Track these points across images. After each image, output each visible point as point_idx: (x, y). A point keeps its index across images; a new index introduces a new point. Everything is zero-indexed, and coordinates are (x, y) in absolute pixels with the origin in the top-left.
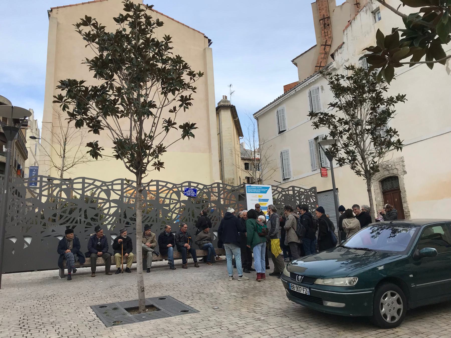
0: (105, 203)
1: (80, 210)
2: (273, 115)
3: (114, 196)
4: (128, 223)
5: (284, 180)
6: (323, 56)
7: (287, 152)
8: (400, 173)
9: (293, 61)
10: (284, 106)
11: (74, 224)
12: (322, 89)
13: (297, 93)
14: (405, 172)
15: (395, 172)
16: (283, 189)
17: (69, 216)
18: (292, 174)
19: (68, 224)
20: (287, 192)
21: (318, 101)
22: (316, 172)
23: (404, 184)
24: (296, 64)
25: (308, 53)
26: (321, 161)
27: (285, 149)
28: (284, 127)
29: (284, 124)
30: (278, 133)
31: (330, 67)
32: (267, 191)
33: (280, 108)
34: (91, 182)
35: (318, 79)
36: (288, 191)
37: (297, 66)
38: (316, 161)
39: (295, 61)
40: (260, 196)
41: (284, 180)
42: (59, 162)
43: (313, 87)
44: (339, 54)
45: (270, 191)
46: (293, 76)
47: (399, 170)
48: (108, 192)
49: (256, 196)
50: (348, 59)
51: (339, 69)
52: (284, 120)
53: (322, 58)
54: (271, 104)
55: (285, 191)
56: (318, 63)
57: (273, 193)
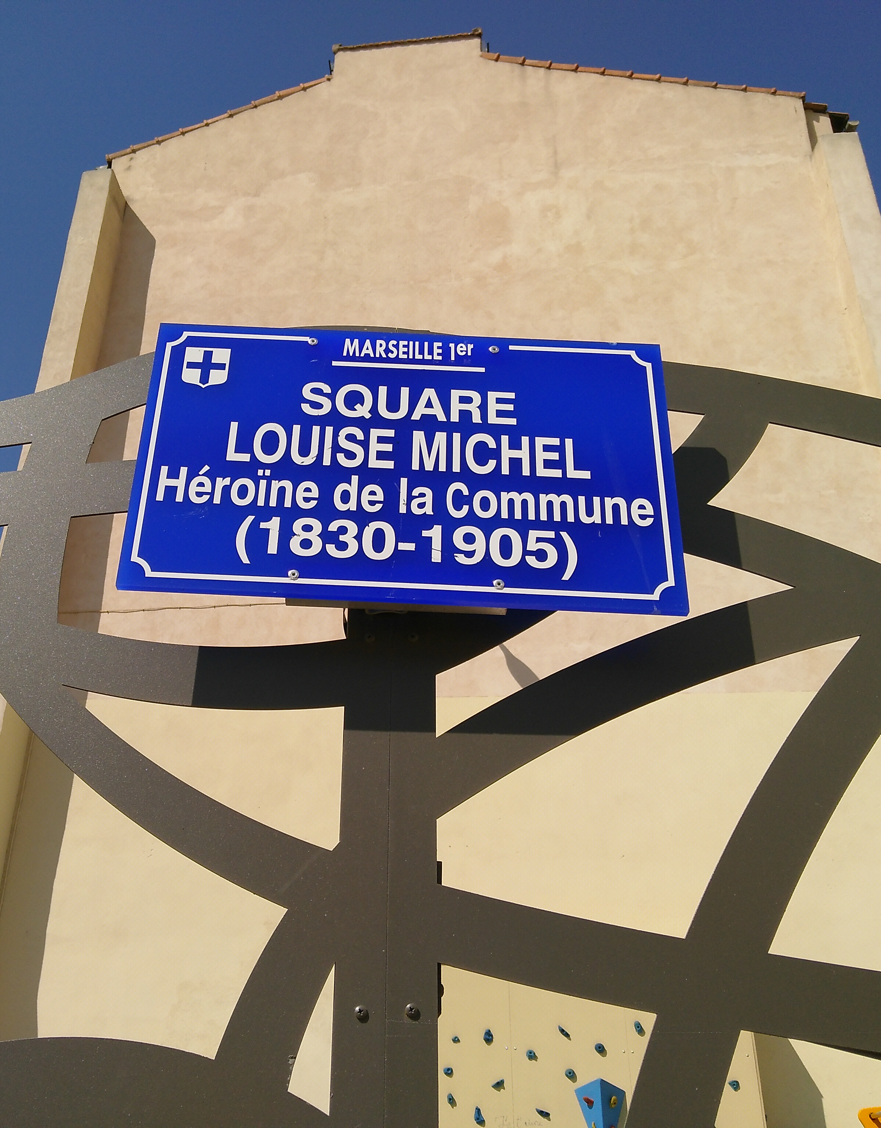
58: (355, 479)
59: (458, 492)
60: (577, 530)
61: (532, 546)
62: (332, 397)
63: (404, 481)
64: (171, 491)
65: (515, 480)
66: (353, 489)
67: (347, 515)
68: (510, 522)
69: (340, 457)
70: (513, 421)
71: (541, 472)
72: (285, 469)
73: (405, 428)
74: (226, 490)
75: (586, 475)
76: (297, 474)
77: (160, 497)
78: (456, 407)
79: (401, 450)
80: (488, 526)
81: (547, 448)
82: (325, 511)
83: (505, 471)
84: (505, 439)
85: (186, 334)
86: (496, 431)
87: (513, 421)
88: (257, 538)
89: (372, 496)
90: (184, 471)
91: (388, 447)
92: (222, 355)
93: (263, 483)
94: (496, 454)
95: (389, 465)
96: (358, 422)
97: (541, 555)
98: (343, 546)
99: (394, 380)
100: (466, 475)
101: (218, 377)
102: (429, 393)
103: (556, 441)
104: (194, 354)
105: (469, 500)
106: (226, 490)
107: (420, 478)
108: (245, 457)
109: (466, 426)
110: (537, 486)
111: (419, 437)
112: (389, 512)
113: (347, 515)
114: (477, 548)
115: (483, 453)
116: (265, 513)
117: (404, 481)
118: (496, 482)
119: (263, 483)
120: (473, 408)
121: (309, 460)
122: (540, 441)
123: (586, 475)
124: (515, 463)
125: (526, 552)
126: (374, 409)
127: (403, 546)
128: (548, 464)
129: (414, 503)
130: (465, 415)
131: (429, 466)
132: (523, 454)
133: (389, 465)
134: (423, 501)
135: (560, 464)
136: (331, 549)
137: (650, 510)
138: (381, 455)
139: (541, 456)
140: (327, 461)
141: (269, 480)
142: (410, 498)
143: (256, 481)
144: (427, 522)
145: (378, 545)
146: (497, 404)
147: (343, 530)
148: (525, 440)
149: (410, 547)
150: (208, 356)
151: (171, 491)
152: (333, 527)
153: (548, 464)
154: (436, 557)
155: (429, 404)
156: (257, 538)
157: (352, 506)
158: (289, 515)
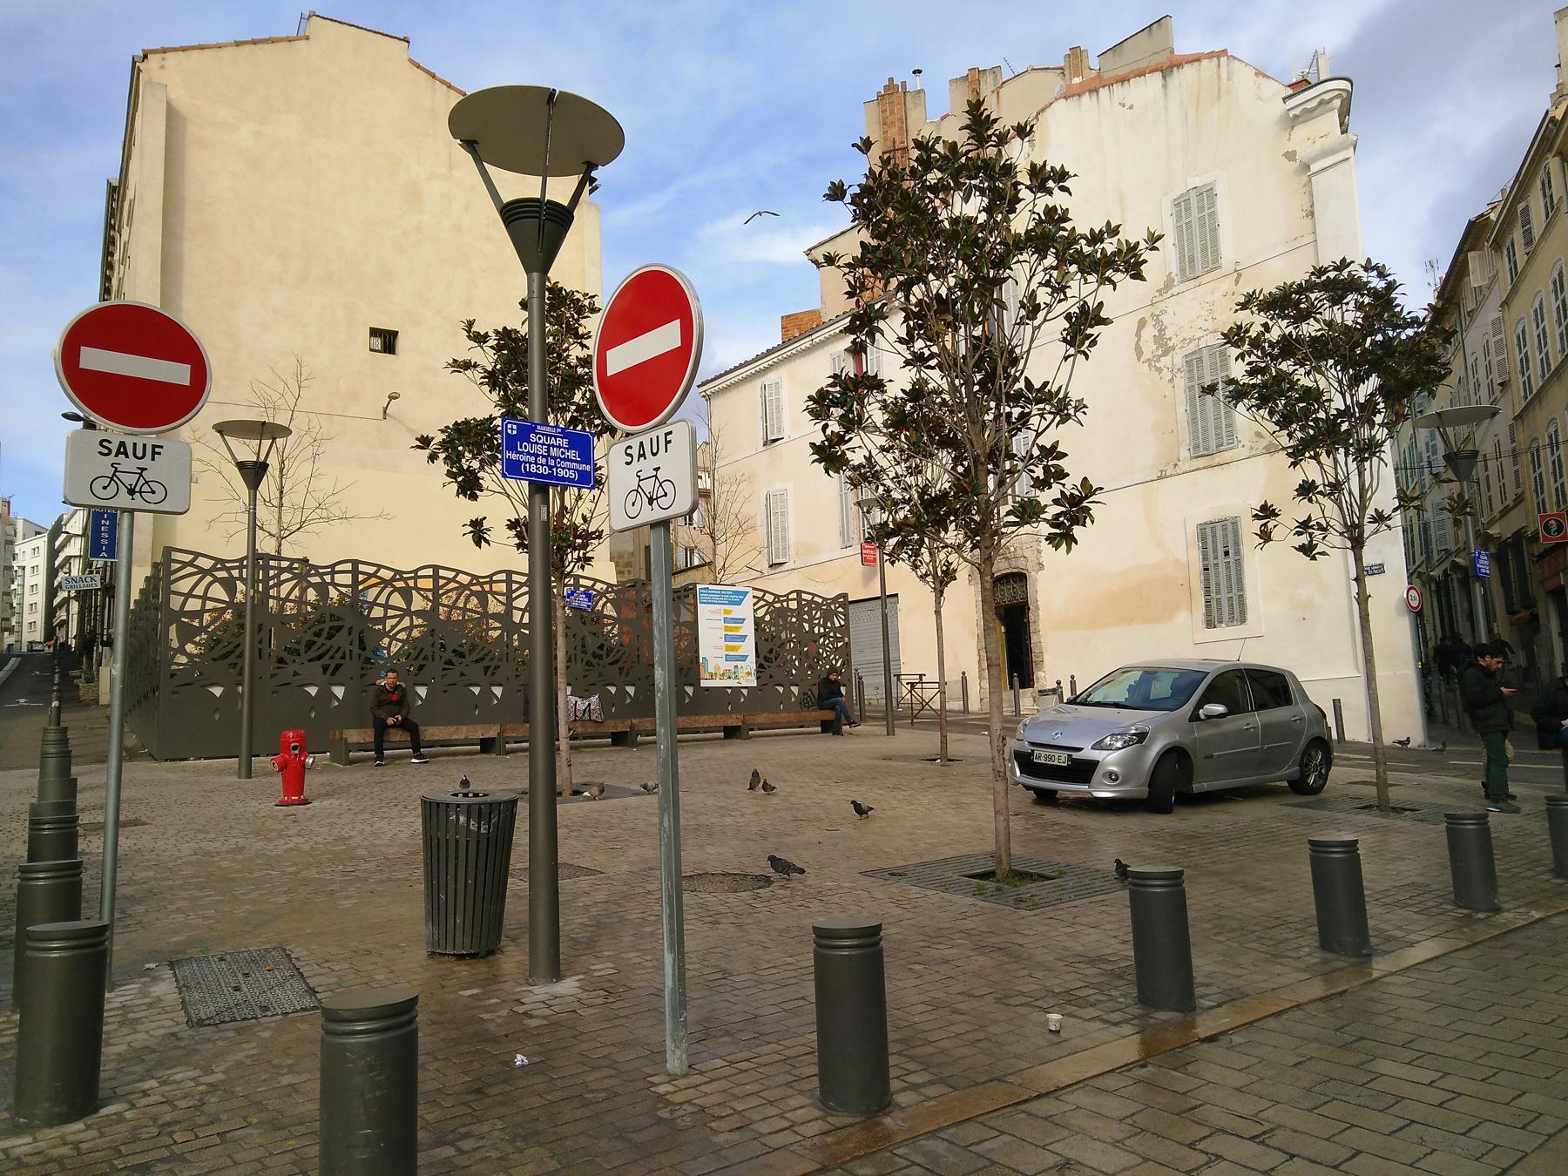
0: (402, 618)
3: (418, 603)
4: (450, 662)
7: (783, 495)
8: (1030, 566)
11: (337, 661)
13: (815, 347)
14: (1041, 566)
15: (1021, 563)
17: (329, 643)
18: (792, 552)
19: (325, 661)
22: (849, 551)
27: (778, 486)
33: (770, 378)
34: (372, 570)
40: (726, 612)
48: (406, 594)
49: (718, 612)
54: (747, 363)
65: (568, 460)
114: (562, 473)
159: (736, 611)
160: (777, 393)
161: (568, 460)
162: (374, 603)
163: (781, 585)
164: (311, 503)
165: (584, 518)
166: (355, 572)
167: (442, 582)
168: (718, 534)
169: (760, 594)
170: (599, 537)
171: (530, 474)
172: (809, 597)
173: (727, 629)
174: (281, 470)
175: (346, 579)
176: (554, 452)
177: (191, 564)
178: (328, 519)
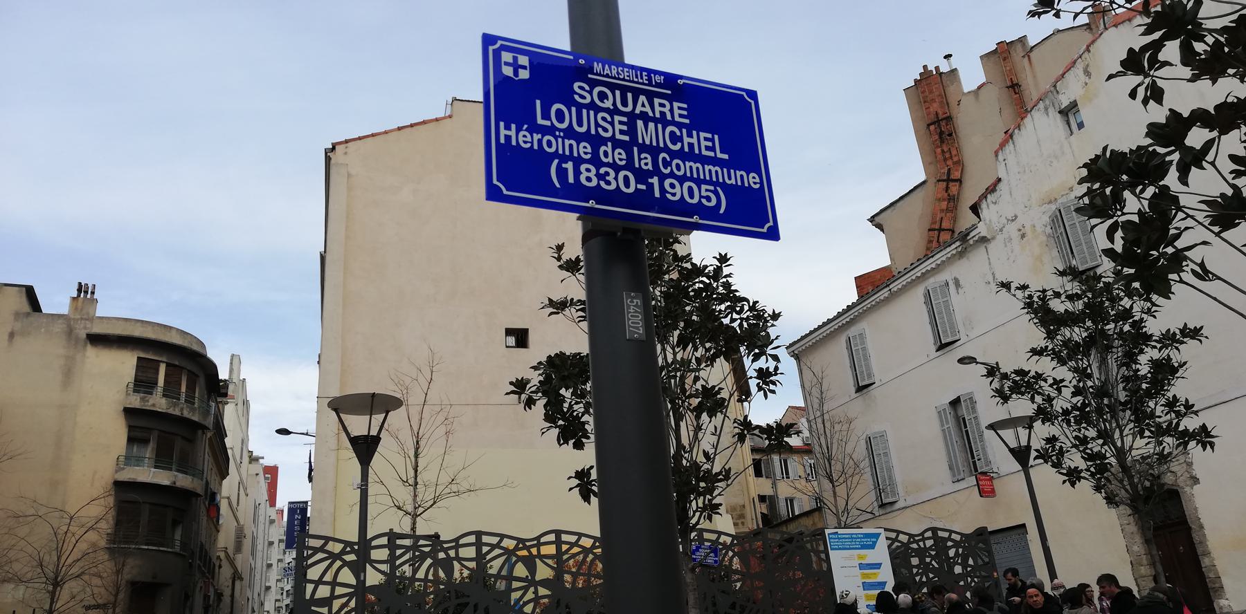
0: (526, 589)
1: (476, 606)
2: (838, 348)
3: (544, 572)
5: (882, 506)
6: (944, 205)
8: (1181, 482)
9: (872, 220)
10: (864, 326)
12: (957, 283)
13: (894, 295)
14: (1195, 480)
16: (911, 536)
18: (900, 490)
20: (921, 544)
21: (950, 313)
23: (1196, 509)
24: (880, 227)
25: (906, 199)
26: (973, 457)
28: (869, 376)
29: (868, 367)
30: (853, 389)
31: (972, 234)
32: (875, 543)
33: (853, 331)
34: (495, 540)
35: (943, 262)
36: (924, 539)
37: (882, 230)
38: (960, 457)
39: (877, 219)
40: (860, 557)
41: (882, 506)
42: (404, 495)
43: (932, 282)
44: (992, 206)
45: (882, 544)
46: (875, 254)
47: (1179, 474)
48: (530, 563)
50: (1016, 217)
51: (993, 238)
52: (866, 358)
53: (942, 211)
54: (829, 321)
55: (917, 542)
56: (934, 223)
57: (889, 547)
58: (609, 144)
59: (664, 159)
60: (724, 186)
61: (704, 194)
62: (590, 92)
63: (635, 149)
64: (508, 138)
65: (689, 155)
66: (609, 150)
67: (608, 165)
68: (691, 179)
69: (600, 130)
70: (687, 121)
71: (705, 152)
72: (570, 133)
73: (632, 117)
74: (540, 141)
75: (726, 157)
76: (579, 138)
77: (502, 141)
78: (658, 109)
79: (632, 131)
80: (682, 180)
81: (706, 139)
82: (596, 161)
83: (686, 149)
84: (684, 131)
85: (500, 43)
86: (680, 126)
87: (687, 121)
88: (562, 173)
89: (620, 156)
90: (513, 126)
91: (625, 128)
92: (523, 60)
93: (560, 140)
94: (681, 139)
95: (626, 138)
96: (606, 110)
97: (709, 199)
98: (608, 183)
99: (624, 90)
100: (666, 149)
101: (524, 74)
102: (642, 98)
103: (710, 136)
104: (507, 57)
105: (669, 164)
106: (540, 141)
107: (643, 148)
108: (548, 123)
109: (663, 121)
110: (705, 160)
111: (640, 123)
112: (629, 166)
113: (608, 165)
114: (677, 192)
115: (675, 138)
116: (564, 159)
117: (635, 149)
118: (680, 155)
119: (560, 140)
120: (666, 110)
121: (583, 129)
122: (702, 135)
123: (726, 157)
124: (691, 145)
125: (701, 197)
126: (614, 104)
127: (640, 186)
128: (707, 148)
129: (643, 162)
130: (663, 114)
131: (648, 142)
132: (694, 140)
133: (626, 138)
134: (646, 163)
135: (712, 149)
136: (602, 184)
137: (758, 180)
138: (622, 132)
139: (704, 143)
140: (593, 132)
141: (563, 139)
142: (640, 160)
143: (556, 138)
144: (651, 174)
145: (627, 185)
146: (678, 110)
147: (607, 174)
148: (694, 133)
149: (643, 187)
150: (515, 59)
151: (508, 138)
152: (602, 171)
153: (707, 148)
154: (657, 194)
155: (643, 105)
156: (562, 173)
157: (610, 160)
158: (578, 161)
159: (871, 556)
160: (863, 343)
161: (689, 155)
162: (498, 576)
163: (911, 524)
164: (445, 479)
165: (706, 455)
166: (478, 544)
167: (565, 547)
168: (835, 477)
169: (893, 535)
170: (727, 477)
171: (578, 191)
172: (946, 535)
173: (865, 576)
174: (417, 449)
175: (470, 552)
176: (647, 134)
177: (321, 549)
178: (457, 493)
